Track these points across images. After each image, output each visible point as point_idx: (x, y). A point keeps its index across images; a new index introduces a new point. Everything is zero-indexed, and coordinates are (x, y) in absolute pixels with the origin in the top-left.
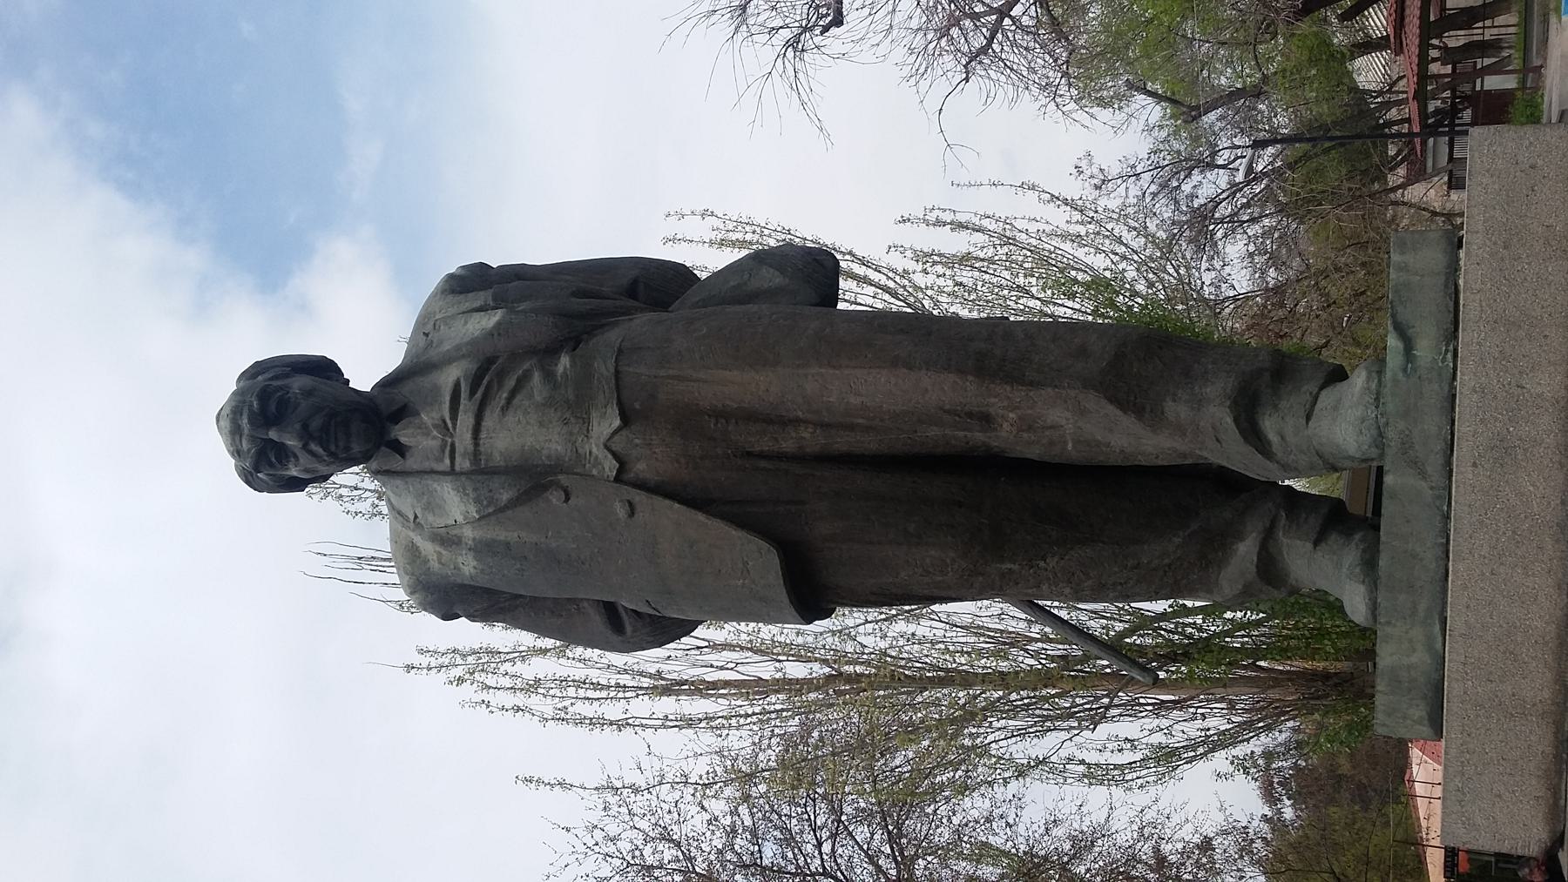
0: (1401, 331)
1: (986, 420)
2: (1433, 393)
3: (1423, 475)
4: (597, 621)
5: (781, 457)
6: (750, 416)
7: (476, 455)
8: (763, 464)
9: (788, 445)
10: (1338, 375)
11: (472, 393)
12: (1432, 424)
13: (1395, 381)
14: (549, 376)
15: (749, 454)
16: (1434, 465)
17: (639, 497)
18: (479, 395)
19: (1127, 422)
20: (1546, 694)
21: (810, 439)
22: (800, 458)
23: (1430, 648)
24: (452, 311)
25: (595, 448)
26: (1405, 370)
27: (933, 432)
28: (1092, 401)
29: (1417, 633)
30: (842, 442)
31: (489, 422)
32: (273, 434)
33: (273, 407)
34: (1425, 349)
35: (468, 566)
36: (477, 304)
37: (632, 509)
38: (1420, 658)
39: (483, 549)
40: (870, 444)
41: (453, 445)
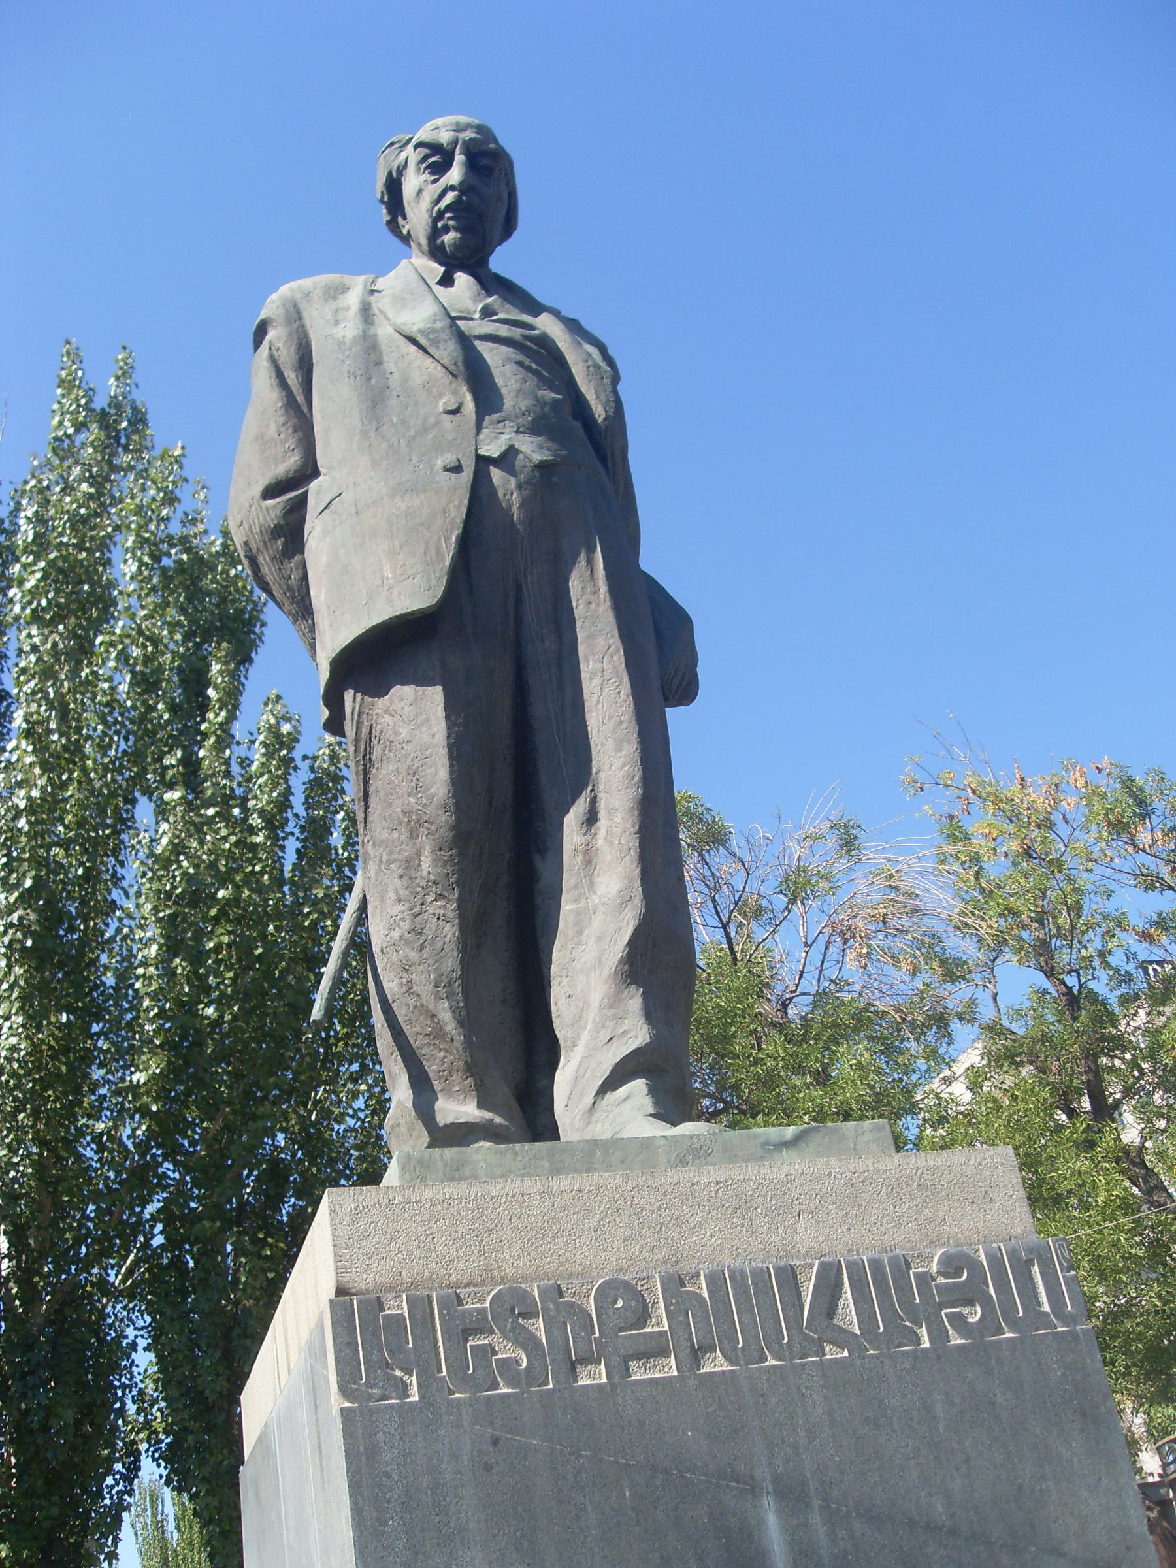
5: (519, 620)
8: (511, 602)
13: (756, 1136)
15: (519, 589)
17: (467, 475)
20: (510, 1271)
26: (766, 1143)
31: (505, 350)
32: (459, 158)
33: (485, 161)
37: (457, 469)
40: (541, 708)
41: (472, 319)
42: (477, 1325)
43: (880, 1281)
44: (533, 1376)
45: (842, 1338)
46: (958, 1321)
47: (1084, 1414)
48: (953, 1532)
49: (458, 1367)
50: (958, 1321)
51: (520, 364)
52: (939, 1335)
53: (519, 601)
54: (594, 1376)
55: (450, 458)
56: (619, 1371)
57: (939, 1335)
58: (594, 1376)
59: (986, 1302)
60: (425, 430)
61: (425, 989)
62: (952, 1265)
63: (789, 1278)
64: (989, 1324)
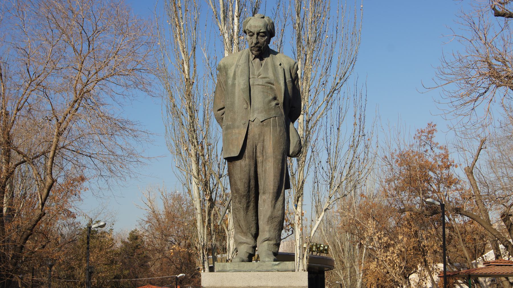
2: (270, 269)
3: (257, 268)
9: (258, 154)
12: (265, 269)
15: (256, 147)
16: (259, 269)
18: (266, 84)
19: (266, 220)
21: (259, 160)
23: (230, 270)
25: (255, 116)
27: (262, 182)
29: (232, 268)
30: (259, 165)
34: (276, 267)
38: (228, 269)
40: (259, 170)
53: (256, 149)
55: (243, 122)
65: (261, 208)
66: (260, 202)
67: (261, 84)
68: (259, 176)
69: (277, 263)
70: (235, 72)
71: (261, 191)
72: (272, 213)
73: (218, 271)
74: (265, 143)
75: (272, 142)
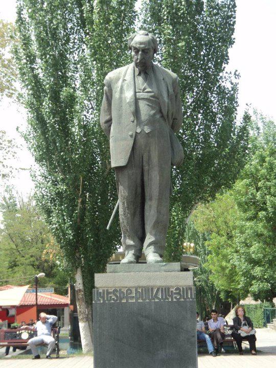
0: (165, 265)
1: (151, 199)
4: (108, 118)
5: (142, 162)
6: (149, 157)
7: (139, 99)
9: (144, 164)
10: (161, 256)
11: (152, 96)
14: (154, 114)
15: (142, 157)
21: (146, 168)
22: (142, 165)
24: (168, 82)
28: (155, 219)
32: (140, 53)
35: (116, 95)
36: (170, 90)
39: (120, 98)
40: (146, 178)
42: (111, 293)
43: (165, 292)
44: (117, 300)
45: (158, 298)
46: (176, 298)
47: (191, 312)
48: (168, 325)
49: (107, 299)
50: (176, 298)
51: (148, 105)
52: (172, 299)
53: (142, 159)
54: (124, 301)
55: (130, 133)
56: (127, 301)
57: (172, 299)
58: (124, 301)
59: (180, 295)
60: (127, 126)
61: (125, 223)
62: (176, 290)
63: (152, 289)
64: (180, 298)
65: (147, 214)
66: (147, 207)
67: (146, 97)
68: (145, 183)
69: (164, 263)
70: (122, 87)
71: (147, 198)
72: (158, 217)
73: (110, 272)
74: (151, 153)
75: (157, 153)
